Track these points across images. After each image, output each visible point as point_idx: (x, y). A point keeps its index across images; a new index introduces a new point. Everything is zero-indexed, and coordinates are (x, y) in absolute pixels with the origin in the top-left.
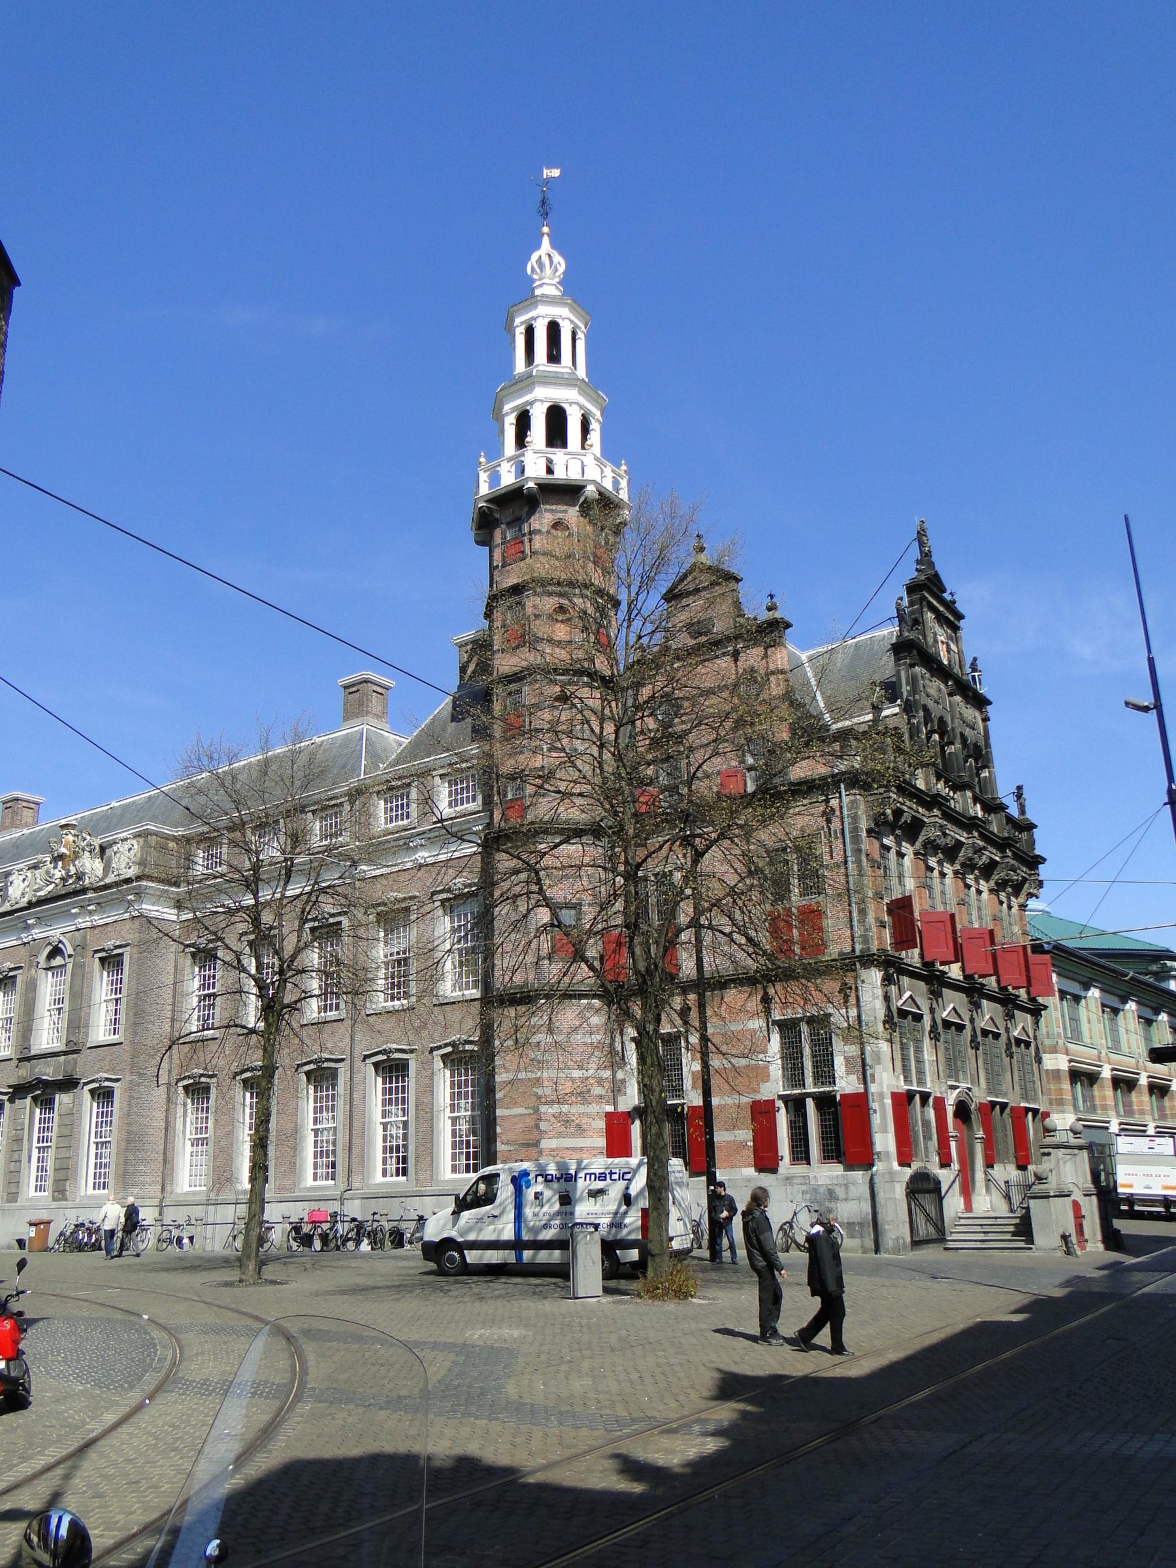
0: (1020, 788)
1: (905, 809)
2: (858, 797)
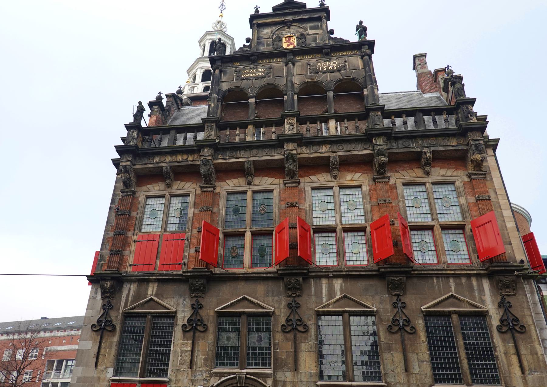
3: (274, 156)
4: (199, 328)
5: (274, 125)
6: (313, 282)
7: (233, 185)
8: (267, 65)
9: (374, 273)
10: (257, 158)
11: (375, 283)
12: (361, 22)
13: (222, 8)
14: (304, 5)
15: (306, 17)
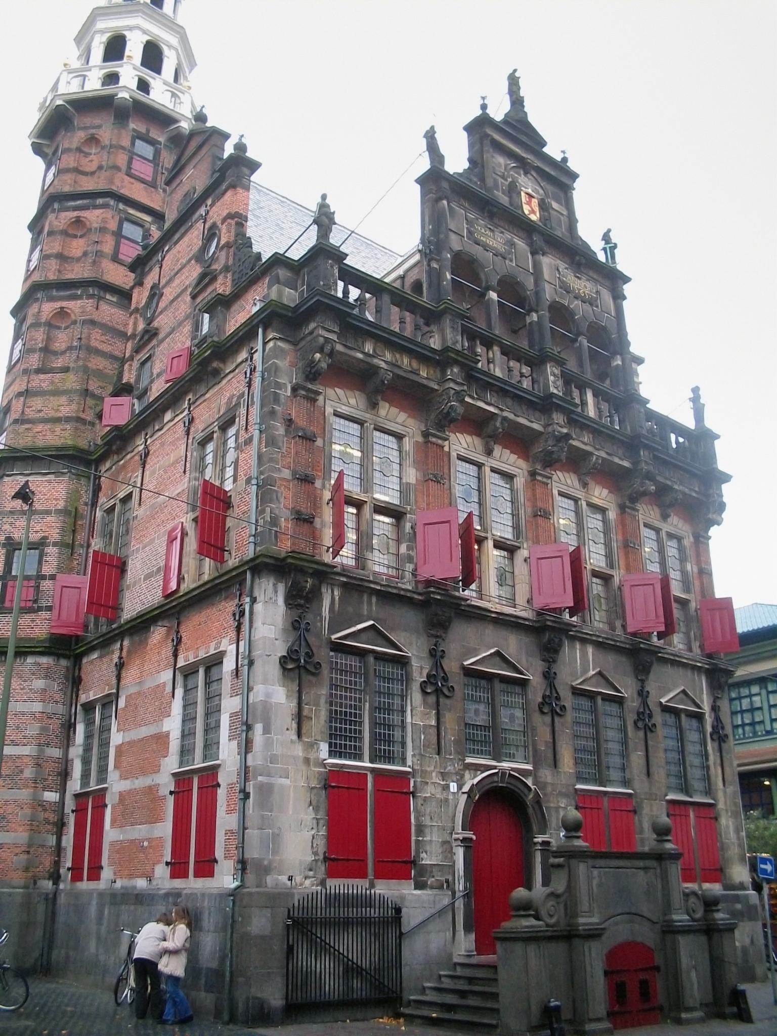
0: (696, 390)
1: (383, 365)
2: (280, 343)
3: (532, 422)
5: (523, 361)
6: (578, 646)
7: (466, 446)
8: (508, 236)
9: (627, 646)
10: (511, 416)
11: (624, 659)
12: (609, 231)
14: (543, 144)
15: (553, 173)
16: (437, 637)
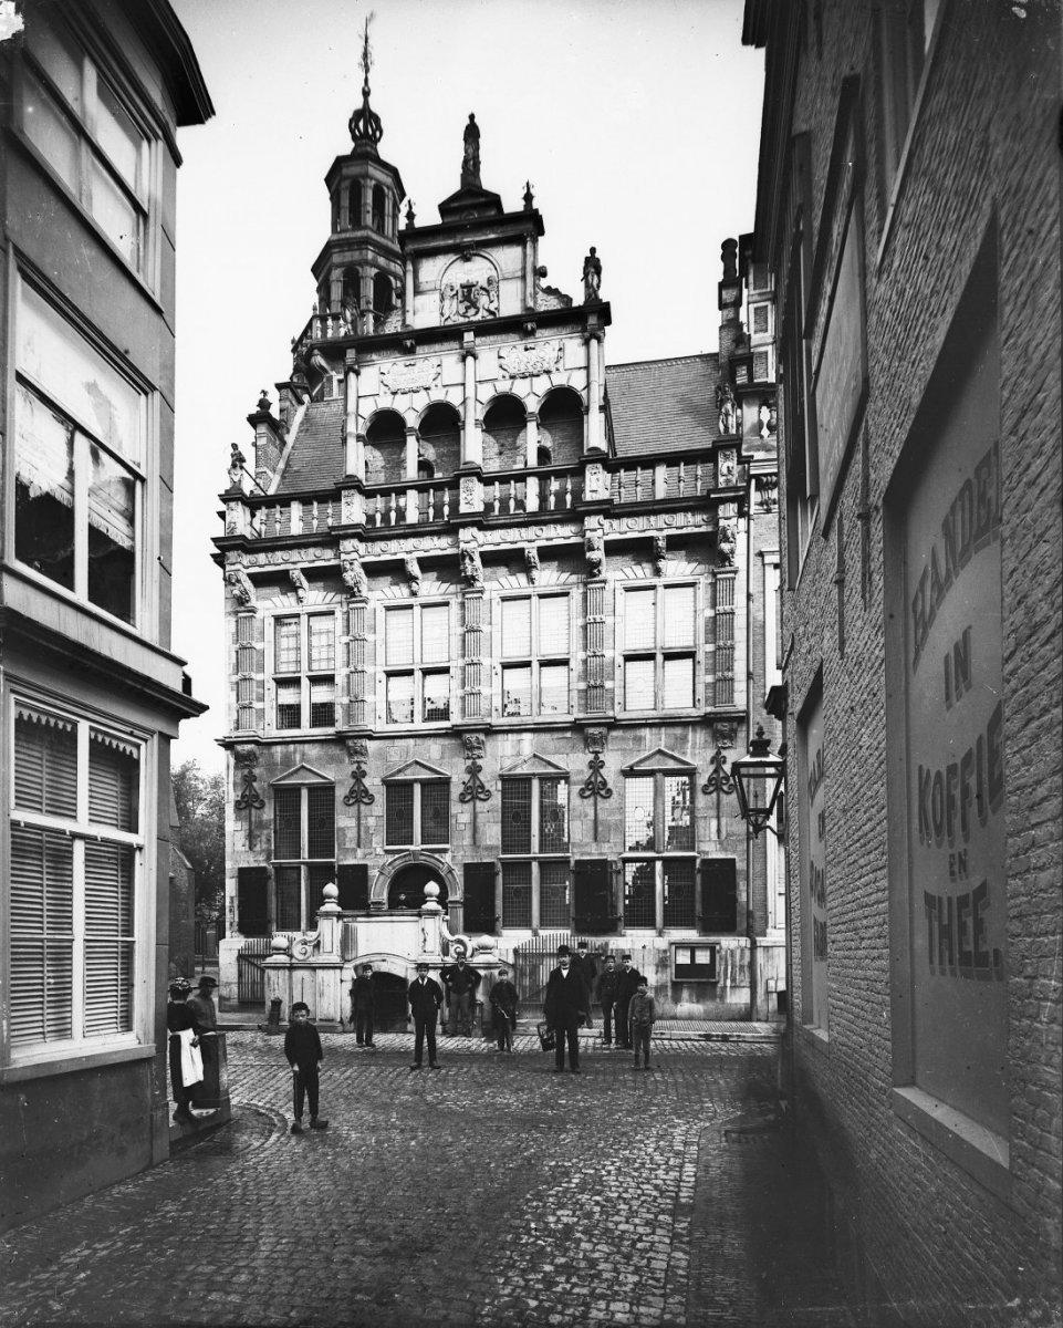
4: (365, 800)
12: (593, 250)
13: (366, 94)
16: (358, 762)
